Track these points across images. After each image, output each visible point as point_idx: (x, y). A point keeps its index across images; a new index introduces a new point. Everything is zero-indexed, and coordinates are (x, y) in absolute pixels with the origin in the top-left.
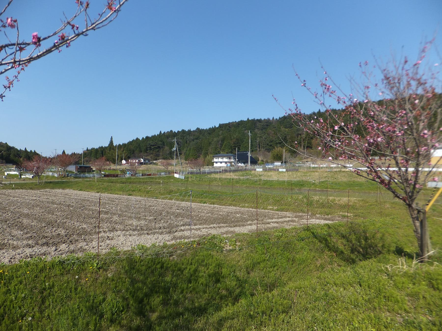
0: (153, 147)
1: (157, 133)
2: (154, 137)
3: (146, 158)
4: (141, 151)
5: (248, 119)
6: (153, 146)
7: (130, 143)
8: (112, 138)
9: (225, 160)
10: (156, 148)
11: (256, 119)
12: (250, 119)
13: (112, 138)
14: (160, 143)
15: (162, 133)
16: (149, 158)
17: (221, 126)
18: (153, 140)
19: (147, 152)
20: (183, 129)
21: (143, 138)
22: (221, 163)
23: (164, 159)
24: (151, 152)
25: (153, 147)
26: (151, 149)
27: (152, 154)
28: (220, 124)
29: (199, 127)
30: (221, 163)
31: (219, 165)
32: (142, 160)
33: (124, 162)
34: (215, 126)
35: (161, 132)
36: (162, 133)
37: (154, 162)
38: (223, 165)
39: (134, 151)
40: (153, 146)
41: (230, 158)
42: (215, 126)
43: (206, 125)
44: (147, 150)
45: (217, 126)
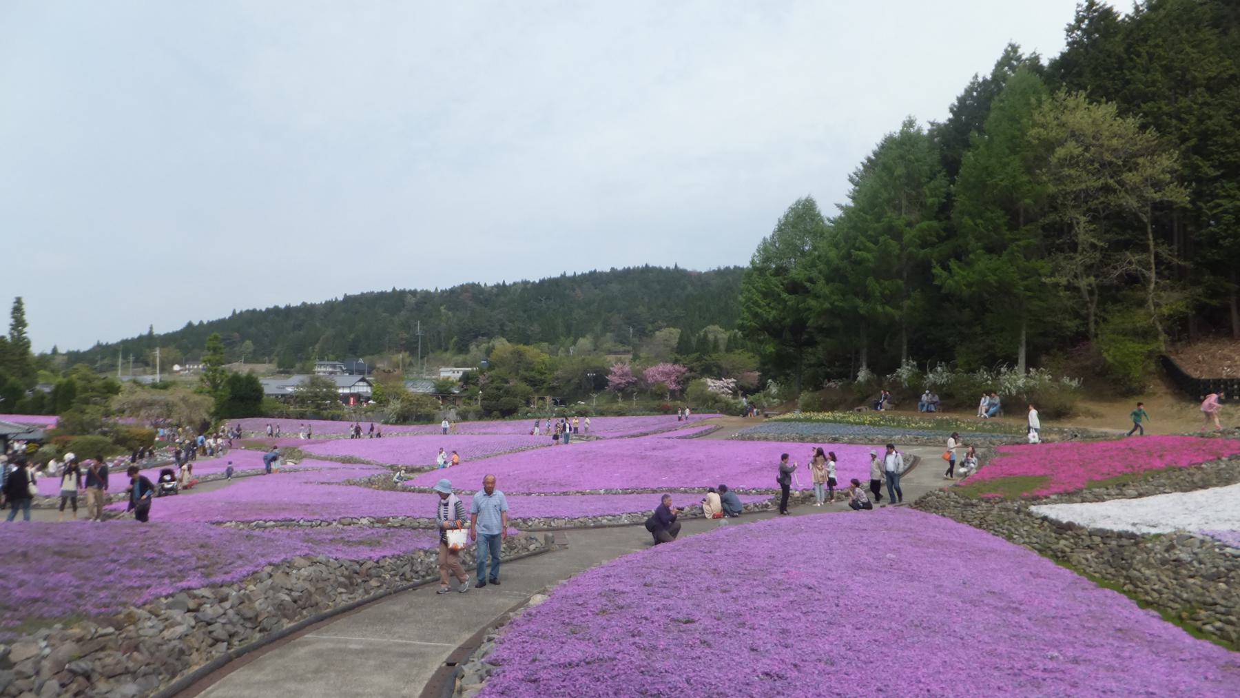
5: (394, 289)
8: (151, 328)
11: (407, 289)
12: (398, 289)
13: (151, 328)
17: (348, 300)
21: (201, 322)
28: (345, 295)
29: (305, 301)
34: (336, 299)
35: (234, 312)
36: (238, 312)
42: (336, 299)
43: (317, 297)
45: (341, 298)
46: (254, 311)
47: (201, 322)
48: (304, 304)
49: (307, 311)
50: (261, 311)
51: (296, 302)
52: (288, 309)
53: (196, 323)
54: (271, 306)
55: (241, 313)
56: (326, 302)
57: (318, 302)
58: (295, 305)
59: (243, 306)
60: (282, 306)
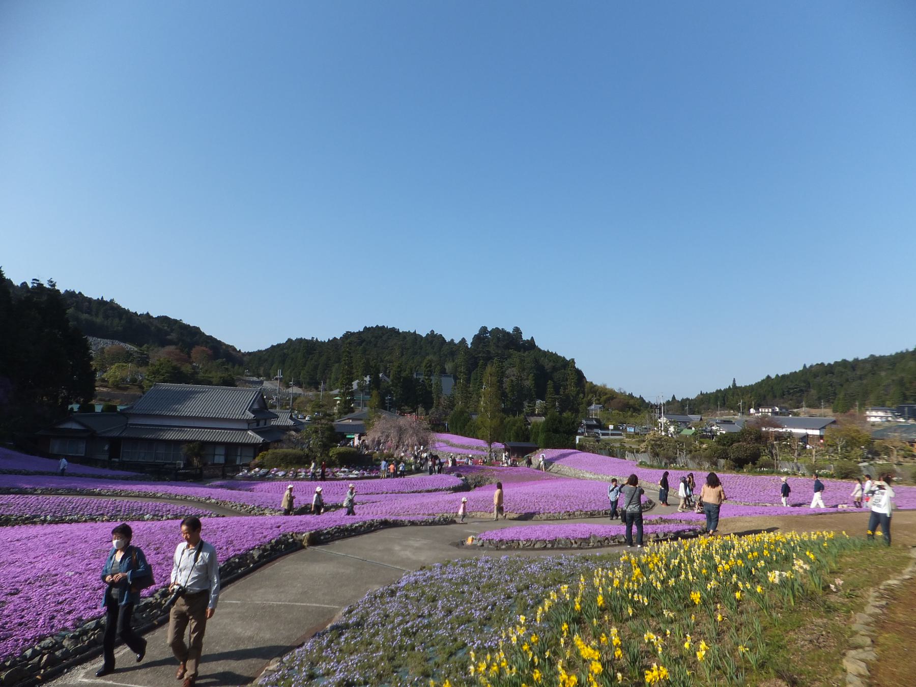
0: (792, 391)
1: (799, 368)
2: (794, 374)
3: (783, 405)
4: (775, 397)
6: (793, 389)
7: (759, 385)
8: (734, 381)
9: (881, 414)
10: (797, 392)
13: (734, 381)
14: (803, 384)
15: (808, 366)
16: (786, 405)
18: (792, 382)
19: (783, 398)
20: (844, 358)
21: (777, 375)
22: (876, 417)
23: (809, 406)
24: (790, 397)
25: (792, 391)
26: (790, 394)
27: (791, 400)
30: (876, 417)
31: (873, 419)
32: (777, 409)
33: (752, 411)
35: (805, 366)
36: (808, 366)
37: (795, 410)
38: (878, 419)
39: (765, 397)
40: (793, 389)
41: (886, 412)
44: (784, 395)
46: (822, 364)
47: (777, 375)
48: (872, 356)
49: (875, 363)
50: (829, 364)
51: (863, 355)
52: (856, 360)
53: (773, 376)
54: (839, 360)
55: (811, 366)
56: (897, 354)
57: (887, 354)
58: (863, 358)
59: (812, 360)
60: (850, 359)
